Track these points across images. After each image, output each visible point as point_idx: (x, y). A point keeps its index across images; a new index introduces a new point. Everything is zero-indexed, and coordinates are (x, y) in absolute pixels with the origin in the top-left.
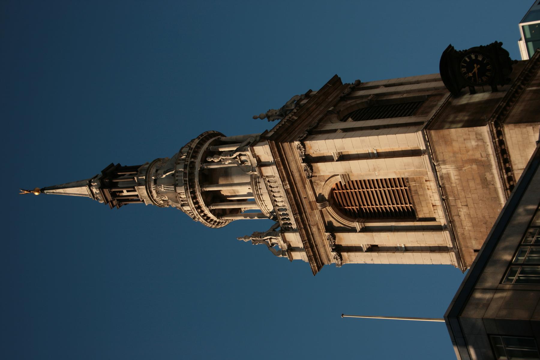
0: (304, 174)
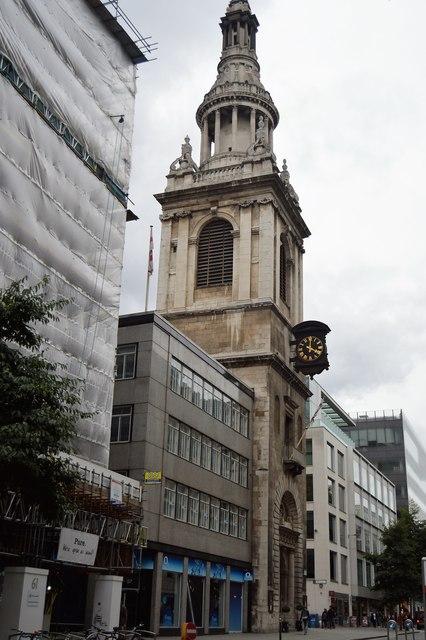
0: (242, 201)
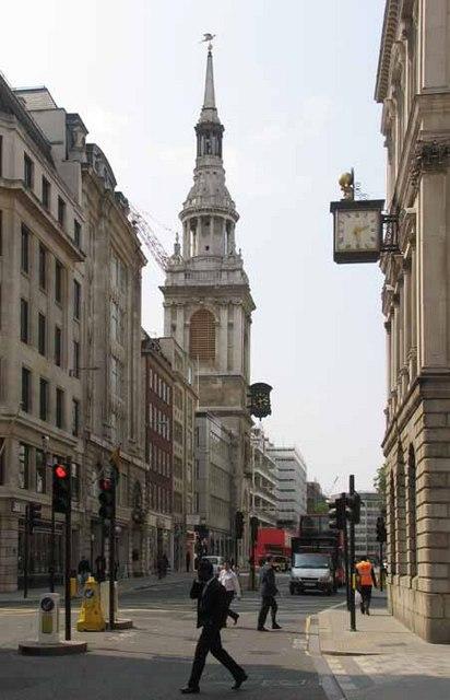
0: (221, 300)
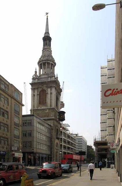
0: (48, 86)
